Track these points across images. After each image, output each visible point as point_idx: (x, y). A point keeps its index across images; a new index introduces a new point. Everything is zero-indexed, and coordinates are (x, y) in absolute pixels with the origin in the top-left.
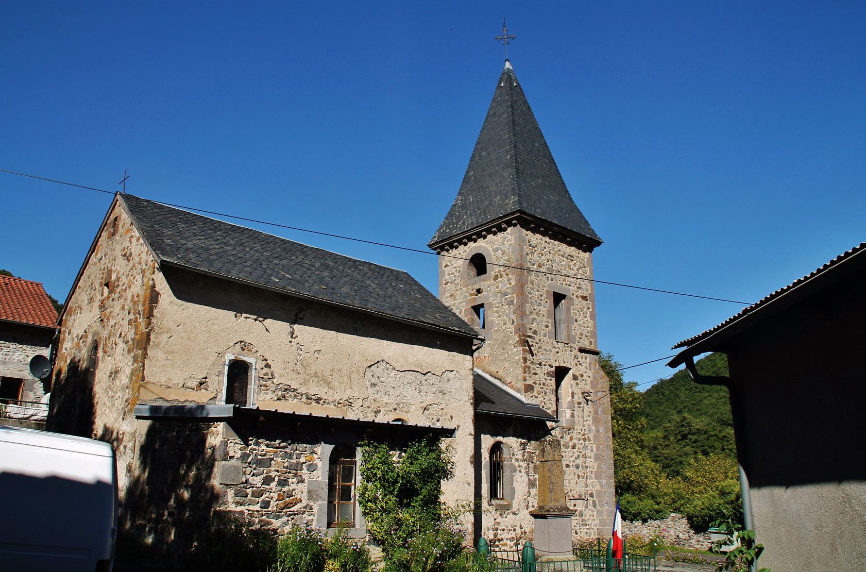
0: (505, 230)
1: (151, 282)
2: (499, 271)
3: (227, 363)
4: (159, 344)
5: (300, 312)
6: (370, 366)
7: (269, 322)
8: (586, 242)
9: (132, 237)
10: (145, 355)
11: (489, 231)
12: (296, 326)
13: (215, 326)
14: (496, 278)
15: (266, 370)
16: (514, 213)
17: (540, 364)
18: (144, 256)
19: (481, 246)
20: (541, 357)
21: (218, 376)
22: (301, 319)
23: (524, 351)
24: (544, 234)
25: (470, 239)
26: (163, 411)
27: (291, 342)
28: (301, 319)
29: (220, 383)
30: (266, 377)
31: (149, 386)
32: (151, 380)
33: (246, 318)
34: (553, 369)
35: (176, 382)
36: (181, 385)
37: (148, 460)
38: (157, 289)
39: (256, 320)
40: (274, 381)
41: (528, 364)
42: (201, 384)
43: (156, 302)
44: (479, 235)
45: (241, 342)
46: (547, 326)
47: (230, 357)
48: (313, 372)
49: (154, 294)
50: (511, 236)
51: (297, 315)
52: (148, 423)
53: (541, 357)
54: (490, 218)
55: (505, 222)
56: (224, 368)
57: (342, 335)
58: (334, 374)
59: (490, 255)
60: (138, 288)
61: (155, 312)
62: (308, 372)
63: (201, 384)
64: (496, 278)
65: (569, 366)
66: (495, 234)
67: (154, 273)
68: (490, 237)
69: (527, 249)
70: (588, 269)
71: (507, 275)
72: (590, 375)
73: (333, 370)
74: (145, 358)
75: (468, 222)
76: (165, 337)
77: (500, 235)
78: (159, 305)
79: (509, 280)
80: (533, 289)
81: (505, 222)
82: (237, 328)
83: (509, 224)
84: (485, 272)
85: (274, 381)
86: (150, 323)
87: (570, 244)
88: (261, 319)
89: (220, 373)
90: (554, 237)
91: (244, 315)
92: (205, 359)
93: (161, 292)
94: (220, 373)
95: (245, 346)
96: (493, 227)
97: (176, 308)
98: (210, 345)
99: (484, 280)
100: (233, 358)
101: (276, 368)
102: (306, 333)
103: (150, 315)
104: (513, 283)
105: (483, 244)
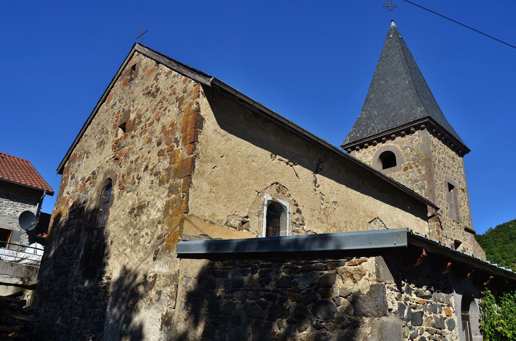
0: (414, 132)
1: (194, 106)
2: (409, 164)
3: (266, 203)
4: (203, 173)
5: (320, 163)
6: (370, 222)
7: (298, 167)
8: (461, 150)
9: (159, 74)
10: (189, 184)
11: (398, 134)
12: (318, 176)
13: (254, 164)
14: (406, 169)
15: (297, 215)
16: (424, 118)
17: (446, 237)
18: (179, 87)
19: (389, 145)
20: (447, 231)
21: (258, 216)
22: (322, 170)
23: (437, 225)
24: (440, 138)
25: (380, 140)
26: (234, 245)
27: (315, 190)
28: (322, 170)
29: (260, 223)
30: (297, 223)
31: (193, 220)
32: (195, 213)
33: (280, 160)
34: (453, 242)
35: (220, 218)
36: (225, 222)
37: (203, 311)
38: (202, 114)
39: (287, 164)
40: (305, 227)
41: (440, 236)
42: (243, 223)
43: (201, 128)
44: (389, 137)
45: (277, 183)
46: (447, 208)
47: (268, 197)
48: (332, 222)
49: (198, 118)
50: (420, 138)
51: (317, 166)
52: (200, 263)
53: (447, 231)
54: (399, 124)
55: (414, 127)
56: (263, 208)
57: (350, 191)
58: (347, 226)
59: (399, 151)
60: (172, 114)
61: (200, 138)
62: (329, 221)
63: (243, 223)
64: (406, 169)
65: (461, 241)
66: (403, 136)
67: (199, 97)
68: (398, 139)
69: (432, 148)
70: (462, 169)
71: (417, 166)
72: (471, 249)
73: (346, 222)
74: (189, 186)
75: (378, 128)
76: (210, 166)
77: (407, 137)
78: (204, 131)
79: (419, 170)
80: (437, 178)
81: (414, 127)
82: (273, 168)
83: (418, 128)
84: (394, 165)
85: (305, 227)
86: (194, 149)
87: (453, 149)
88: (291, 164)
89: (259, 214)
90: (444, 142)
91: (278, 157)
92: (247, 196)
93: (206, 118)
94: (259, 214)
95: (280, 188)
96: (402, 130)
97: (219, 137)
98: (251, 182)
99: (394, 171)
100: (270, 198)
101: (306, 214)
102: (327, 184)
103: (194, 142)
104: (424, 172)
105: (392, 144)
